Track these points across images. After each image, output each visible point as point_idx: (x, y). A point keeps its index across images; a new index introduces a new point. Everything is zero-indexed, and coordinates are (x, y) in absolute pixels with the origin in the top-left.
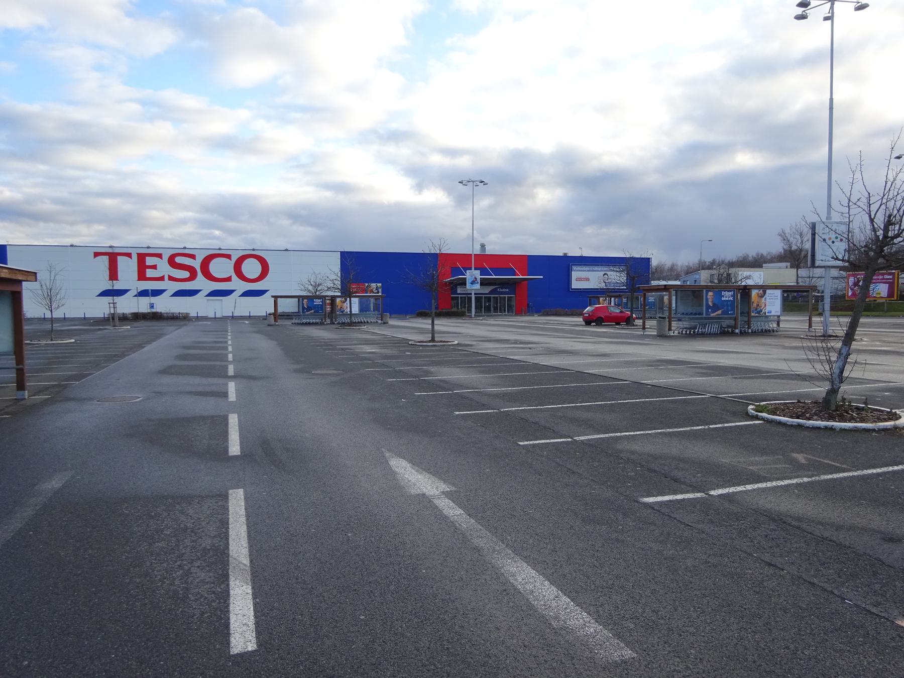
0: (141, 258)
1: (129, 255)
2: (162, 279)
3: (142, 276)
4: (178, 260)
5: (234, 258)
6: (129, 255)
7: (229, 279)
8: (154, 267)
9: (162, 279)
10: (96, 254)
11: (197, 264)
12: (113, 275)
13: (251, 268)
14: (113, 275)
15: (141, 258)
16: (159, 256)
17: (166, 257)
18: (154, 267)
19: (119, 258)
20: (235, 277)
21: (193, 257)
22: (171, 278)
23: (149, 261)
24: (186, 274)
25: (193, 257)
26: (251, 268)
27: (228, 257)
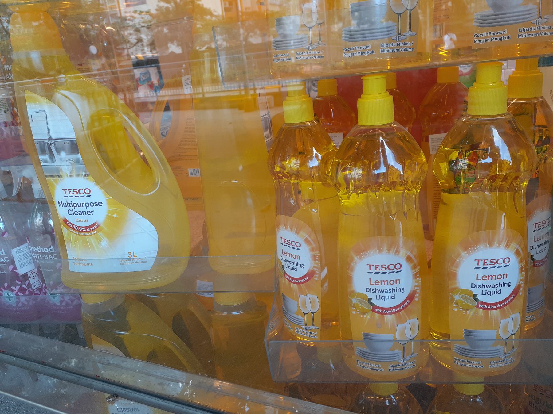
0: (376, 266)
1: (373, 265)
2: (379, 270)
3: (376, 270)
4: (383, 266)
5: (394, 265)
6: (373, 265)
7: (393, 269)
8: (378, 268)
9: (379, 270)
10: (367, 265)
11: (387, 267)
12: (370, 269)
13: (398, 266)
14: (370, 269)
15: (376, 266)
16: (379, 265)
17: (380, 266)
18: (378, 268)
19: (371, 266)
20: (394, 269)
21: (386, 265)
22: (381, 270)
23: (377, 266)
24: (384, 269)
25: (386, 265)
26: (398, 266)
27: (393, 265)
